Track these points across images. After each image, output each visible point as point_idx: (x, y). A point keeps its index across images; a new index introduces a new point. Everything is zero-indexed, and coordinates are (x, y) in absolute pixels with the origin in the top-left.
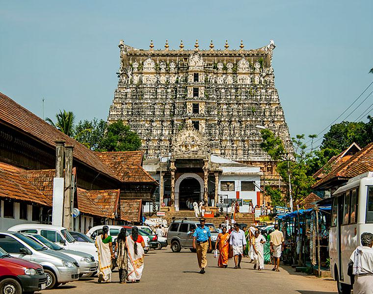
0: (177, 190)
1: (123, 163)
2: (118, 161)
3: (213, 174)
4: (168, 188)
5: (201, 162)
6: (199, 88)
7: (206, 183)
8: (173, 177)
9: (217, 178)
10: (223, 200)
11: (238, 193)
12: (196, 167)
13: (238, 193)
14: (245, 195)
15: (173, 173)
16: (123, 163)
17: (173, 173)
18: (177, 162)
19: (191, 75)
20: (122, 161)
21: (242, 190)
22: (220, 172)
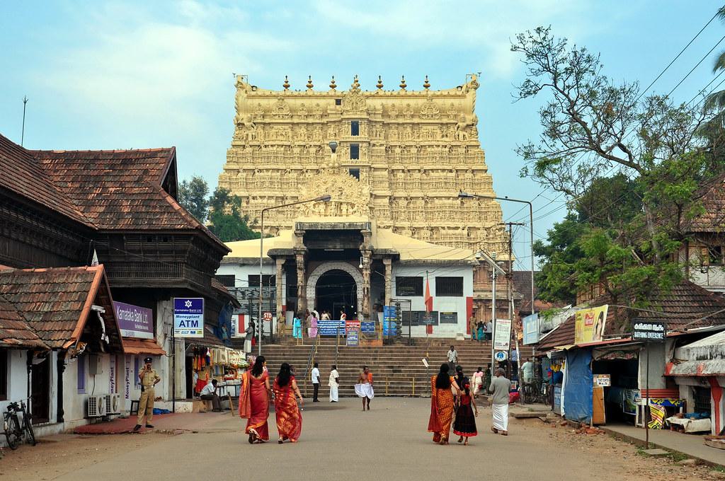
0: (311, 293)
1: (110, 179)
2: (96, 173)
3: (381, 261)
4: (292, 291)
5: (354, 235)
6: (360, 145)
7: (367, 279)
8: (302, 266)
9: (388, 270)
10: (401, 316)
11: (429, 302)
12: (347, 247)
13: (429, 302)
14: (445, 304)
15: (300, 259)
16: (110, 179)
17: (300, 259)
18: (311, 235)
19: (347, 125)
20: (107, 175)
21: (436, 296)
22: (395, 258)
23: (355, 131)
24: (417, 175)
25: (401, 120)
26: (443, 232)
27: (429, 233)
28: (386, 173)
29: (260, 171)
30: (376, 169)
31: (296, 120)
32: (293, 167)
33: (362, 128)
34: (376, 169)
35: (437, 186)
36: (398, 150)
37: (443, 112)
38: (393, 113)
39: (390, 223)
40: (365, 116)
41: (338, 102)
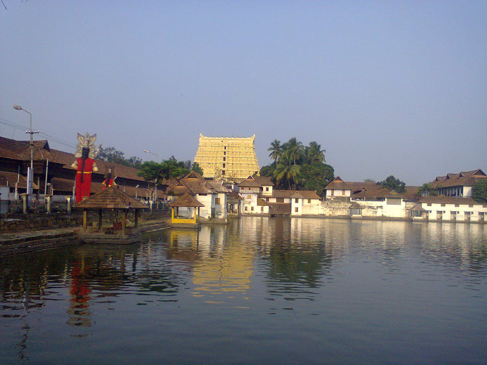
23: (225, 148)
24: (239, 159)
25: (236, 146)
26: (244, 172)
27: (240, 172)
28: (232, 158)
29: (204, 157)
30: (229, 157)
31: (212, 145)
32: (211, 156)
33: (226, 148)
34: (229, 157)
35: (242, 161)
36: (235, 153)
37: (245, 144)
38: (234, 144)
39: (232, 170)
40: (227, 145)
41: (222, 141)
